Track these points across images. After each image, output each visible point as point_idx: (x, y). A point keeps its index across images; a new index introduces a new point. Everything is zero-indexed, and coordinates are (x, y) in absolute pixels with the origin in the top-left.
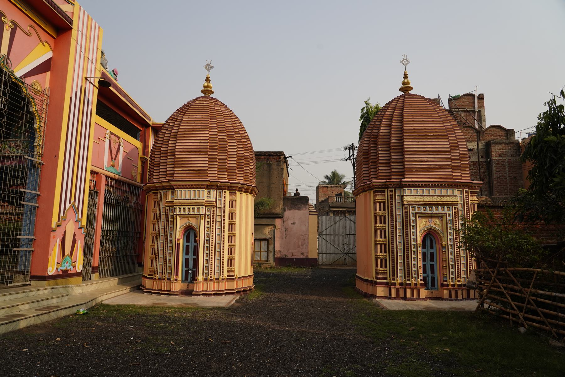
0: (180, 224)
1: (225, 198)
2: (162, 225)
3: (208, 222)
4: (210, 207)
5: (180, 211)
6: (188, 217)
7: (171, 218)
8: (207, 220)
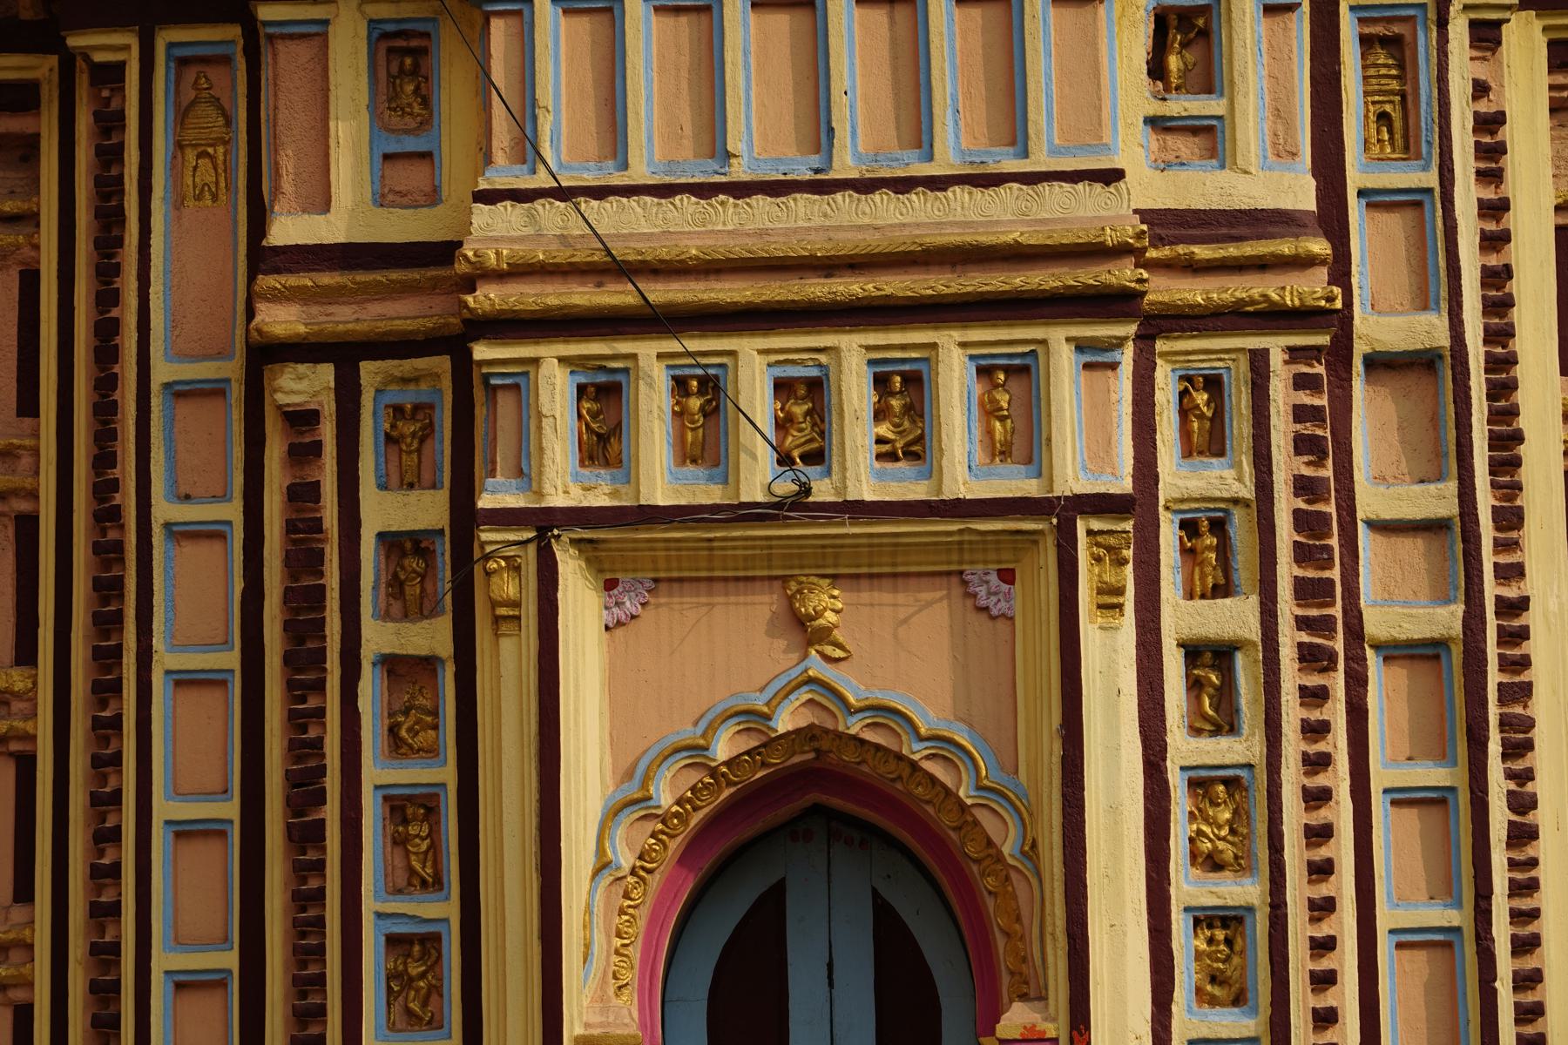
0: (622, 713)
1: (1491, 155)
2: (187, 767)
3: (1211, 657)
4: (1223, 351)
5: (603, 444)
6: (782, 575)
7: (405, 601)
8: (1182, 618)
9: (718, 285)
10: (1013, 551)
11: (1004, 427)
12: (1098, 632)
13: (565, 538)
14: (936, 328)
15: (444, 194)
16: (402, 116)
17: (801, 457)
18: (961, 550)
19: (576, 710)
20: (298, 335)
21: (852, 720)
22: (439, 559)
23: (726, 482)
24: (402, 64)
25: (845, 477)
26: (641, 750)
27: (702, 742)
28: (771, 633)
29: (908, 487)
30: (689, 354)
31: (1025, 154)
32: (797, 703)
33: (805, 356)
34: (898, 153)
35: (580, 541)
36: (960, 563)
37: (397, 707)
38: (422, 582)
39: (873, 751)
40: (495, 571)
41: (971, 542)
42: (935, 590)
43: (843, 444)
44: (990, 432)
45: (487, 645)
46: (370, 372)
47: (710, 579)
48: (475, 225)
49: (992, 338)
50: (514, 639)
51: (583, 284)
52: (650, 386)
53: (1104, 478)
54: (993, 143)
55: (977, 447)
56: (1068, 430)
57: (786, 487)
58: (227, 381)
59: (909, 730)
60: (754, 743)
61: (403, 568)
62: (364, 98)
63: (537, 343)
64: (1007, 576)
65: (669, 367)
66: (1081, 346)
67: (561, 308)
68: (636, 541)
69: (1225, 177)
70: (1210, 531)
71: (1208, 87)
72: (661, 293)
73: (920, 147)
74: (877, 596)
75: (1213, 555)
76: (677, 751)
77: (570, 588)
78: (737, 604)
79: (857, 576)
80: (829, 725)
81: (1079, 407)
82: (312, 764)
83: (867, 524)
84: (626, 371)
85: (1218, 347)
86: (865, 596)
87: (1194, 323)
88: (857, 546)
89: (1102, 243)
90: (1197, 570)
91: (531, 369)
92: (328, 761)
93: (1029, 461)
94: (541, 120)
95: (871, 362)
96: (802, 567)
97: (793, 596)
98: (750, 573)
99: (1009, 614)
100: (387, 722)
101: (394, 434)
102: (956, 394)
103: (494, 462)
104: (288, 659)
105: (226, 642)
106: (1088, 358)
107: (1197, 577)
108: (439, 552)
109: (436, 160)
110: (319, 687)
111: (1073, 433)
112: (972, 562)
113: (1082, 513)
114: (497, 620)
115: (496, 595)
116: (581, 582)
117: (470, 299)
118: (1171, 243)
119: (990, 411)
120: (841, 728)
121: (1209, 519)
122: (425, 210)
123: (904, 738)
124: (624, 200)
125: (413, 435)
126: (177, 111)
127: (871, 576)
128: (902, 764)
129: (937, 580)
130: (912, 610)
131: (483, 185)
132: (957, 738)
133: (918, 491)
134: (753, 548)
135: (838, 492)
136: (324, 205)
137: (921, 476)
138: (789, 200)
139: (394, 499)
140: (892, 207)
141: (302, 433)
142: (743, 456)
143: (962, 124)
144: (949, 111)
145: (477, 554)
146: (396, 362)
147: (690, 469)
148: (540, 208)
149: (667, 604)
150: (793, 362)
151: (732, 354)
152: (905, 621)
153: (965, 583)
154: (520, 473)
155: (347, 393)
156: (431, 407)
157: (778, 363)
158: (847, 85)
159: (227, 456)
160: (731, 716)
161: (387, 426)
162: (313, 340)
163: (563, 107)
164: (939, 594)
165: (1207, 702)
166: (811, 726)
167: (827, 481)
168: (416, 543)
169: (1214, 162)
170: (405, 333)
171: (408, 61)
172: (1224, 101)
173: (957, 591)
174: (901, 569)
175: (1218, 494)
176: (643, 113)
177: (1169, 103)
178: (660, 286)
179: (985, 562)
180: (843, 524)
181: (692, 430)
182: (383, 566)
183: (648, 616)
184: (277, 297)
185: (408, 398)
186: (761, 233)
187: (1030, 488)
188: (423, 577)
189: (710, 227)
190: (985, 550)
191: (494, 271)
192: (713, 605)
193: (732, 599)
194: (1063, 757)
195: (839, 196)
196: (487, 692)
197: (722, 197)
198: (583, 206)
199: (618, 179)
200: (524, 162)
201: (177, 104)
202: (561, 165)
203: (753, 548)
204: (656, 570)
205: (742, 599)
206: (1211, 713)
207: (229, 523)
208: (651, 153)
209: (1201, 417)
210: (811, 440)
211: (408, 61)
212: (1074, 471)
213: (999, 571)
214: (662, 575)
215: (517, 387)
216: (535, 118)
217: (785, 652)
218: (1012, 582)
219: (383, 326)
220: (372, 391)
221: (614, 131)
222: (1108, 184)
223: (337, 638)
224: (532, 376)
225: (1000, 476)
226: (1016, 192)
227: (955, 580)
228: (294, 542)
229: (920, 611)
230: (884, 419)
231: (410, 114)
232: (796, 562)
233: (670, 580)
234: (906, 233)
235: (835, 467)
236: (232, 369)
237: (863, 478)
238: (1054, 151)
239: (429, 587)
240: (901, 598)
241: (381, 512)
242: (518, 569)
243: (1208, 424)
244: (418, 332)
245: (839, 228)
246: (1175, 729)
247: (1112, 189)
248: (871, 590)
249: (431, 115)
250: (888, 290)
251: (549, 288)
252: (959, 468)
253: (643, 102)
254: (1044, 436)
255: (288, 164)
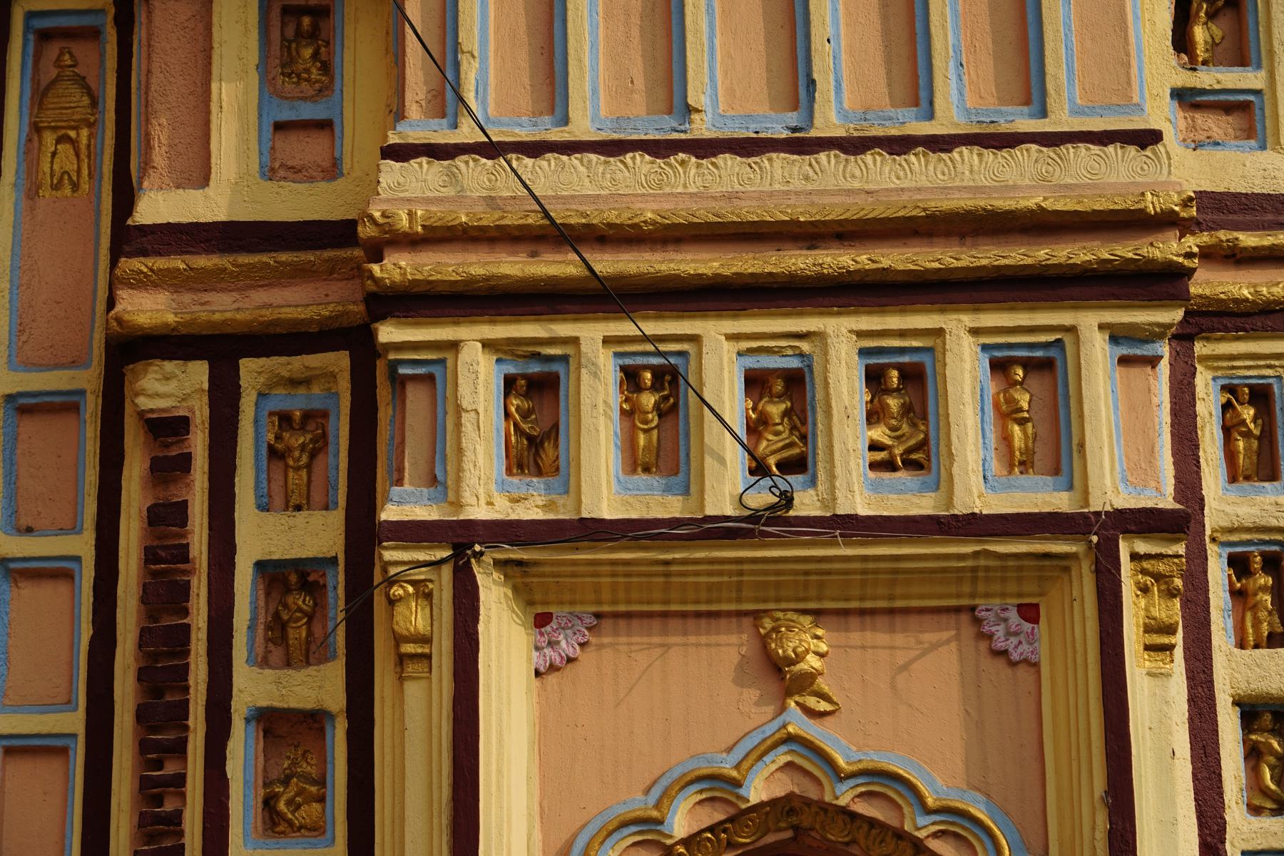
5: (537, 445)
9: (679, 257)
10: (1034, 581)
11: (1025, 432)
12: (1147, 678)
13: (488, 559)
14: (942, 311)
15: (346, 166)
16: (298, 83)
17: (778, 465)
18: (974, 580)
19: (500, 772)
20: (166, 325)
21: (842, 787)
22: (331, 594)
23: (686, 492)
24: (299, 25)
25: (833, 488)
26: (578, 825)
27: (655, 814)
28: (740, 681)
29: (907, 498)
30: (646, 338)
31: (1043, 113)
32: (774, 767)
33: (783, 343)
34: (892, 112)
35: (507, 562)
36: (973, 596)
37: (274, 774)
38: (309, 623)
39: (865, 827)
40: (400, 599)
41: (987, 569)
42: (940, 630)
43: (830, 447)
44: (1006, 439)
45: (388, 692)
46: (251, 371)
47: (665, 615)
48: (384, 184)
49: (1011, 324)
50: (423, 683)
51: (514, 253)
52: (595, 375)
53: (1147, 492)
54: (1002, 101)
55: (992, 454)
56: (1105, 438)
57: (761, 498)
58: (82, 393)
59: (912, 800)
60: (719, 816)
61: (286, 606)
62: (253, 56)
63: (457, 323)
64: (1030, 613)
65: (617, 355)
66: (1117, 335)
67: (487, 279)
68: (575, 563)
69: (1267, 158)
70: (1263, 569)
71: (1241, 57)
72: (608, 263)
73: (917, 105)
74: (870, 637)
75: (1268, 598)
76: (624, 824)
77: (494, 619)
78: (698, 645)
79: (845, 613)
80: (813, 794)
81: (1116, 408)
82: (168, 843)
83: (862, 544)
84: (564, 359)
85: (1267, 351)
86: (855, 637)
87: (1239, 322)
88: (847, 572)
89: (1142, 211)
90: (1249, 616)
91: (449, 356)
92: (187, 840)
93: (1056, 471)
94: (464, 67)
95: (863, 352)
96: (778, 600)
97: (768, 635)
98: (714, 608)
99: (1033, 659)
100: (261, 792)
101: (280, 446)
102: (967, 389)
103: (401, 470)
104: (142, 715)
105: (69, 702)
106: (1124, 351)
107: (1249, 624)
108: (330, 585)
109: (337, 129)
110: (179, 749)
111: (1110, 437)
112: (987, 595)
113: (1126, 532)
114: (402, 659)
115: (401, 626)
116: (506, 614)
117: (376, 268)
118: (1210, 229)
119: (1008, 413)
120: (828, 798)
121: (1262, 554)
122: (323, 185)
123: (906, 810)
124: (565, 158)
125: (303, 447)
126: (35, 90)
127: (862, 612)
128: (902, 844)
129: (944, 618)
130: (914, 654)
131: (393, 139)
132: (972, 810)
133: (924, 505)
134: (721, 573)
135: (824, 505)
136: (202, 177)
137: (925, 488)
138: (764, 160)
139: (276, 520)
140: (887, 169)
141: (167, 446)
142: (708, 460)
143: (965, 78)
144: (952, 64)
145: (378, 578)
146: (284, 359)
147: (641, 478)
148: (462, 166)
149: (611, 645)
150: (768, 351)
151: (695, 339)
152: (905, 667)
153: (978, 621)
154: (433, 481)
155: (224, 396)
156: (325, 414)
157: (750, 351)
158: (830, 31)
159: (77, 481)
160: (691, 782)
161: (271, 437)
162: (184, 331)
163: (491, 54)
164: (945, 635)
165: (1267, 774)
166: (790, 797)
167: (811, 492)
168: (303, 576)
169: (1253, 143)
170: (296, 322)
171: (306, 21)
172: (1262, 74)
173: (968, 631)
174: (899, 604)
175: (1274, 523)
176: (587, 62)
177: (1199, 74)
178: (607, 257)
179: (1003, 595)
180: (833, 544)
181: (645, 431)
182: (262, 603)
183: (588, 659)
184: (142, 283)
185: (296, 403)
186: (730, 197)
187: (1061, 502)
188: (311, 618)
189: (667, 190)
190: (1004, 580)
191: (406, 235)
192: (667, 647)
193: (692, 639)
194: (1109, 832)
195: (822, 156)
196: (387, 750)
197: (681, 156)
198: (515, 164)
199: (556, 135)
200: (444, 116)
201: (36, 81)
202: (487, 118)
203: (721, 573)
204: (599, 602)
205: (703, 639)
206: (1273, 787)
207: (77, 559)
208: (596, 108)
209: (1248, 435)
210: (791, 445)
211: (306, 21)
212: (1114, 483)
213: (1019, 606)
214: (606, 608)
215: (430, 378)
216: (457, 65)
217: (757, 704)
218: (1036, 620)
219: (269, 315)
220: (254, 396)
221: (552, 84)
222: (1143, 147)
223: (203, 687)
224: (450, 364)
225: (1022, 488)
226: (1034, 155)
227: (965, 618)
228: (155, 574)
229: (923, 655)
230: (878, 422)
231: (308, 80)
232: (772, 593)
233: (616, 615)
234: (905, 197)
235: (822, 475)
236: (89, 379)
237: (856, 488)
238: (1077, 111)
239: (318, 630)
240: (899, 639)
241: (261, 536)
242: (428, 596)
243: (1255, 444)
244: (311, 321)
245: (822, 192)
246: (1233, 804)
247: (1148, 152)
248: (863, 629)
249: (332, 80)
250: (885, 263)
251: (472, 257)
252: (973, 478)
253: (587, 48)
254: (1075, 441)
255: (161, 134)
